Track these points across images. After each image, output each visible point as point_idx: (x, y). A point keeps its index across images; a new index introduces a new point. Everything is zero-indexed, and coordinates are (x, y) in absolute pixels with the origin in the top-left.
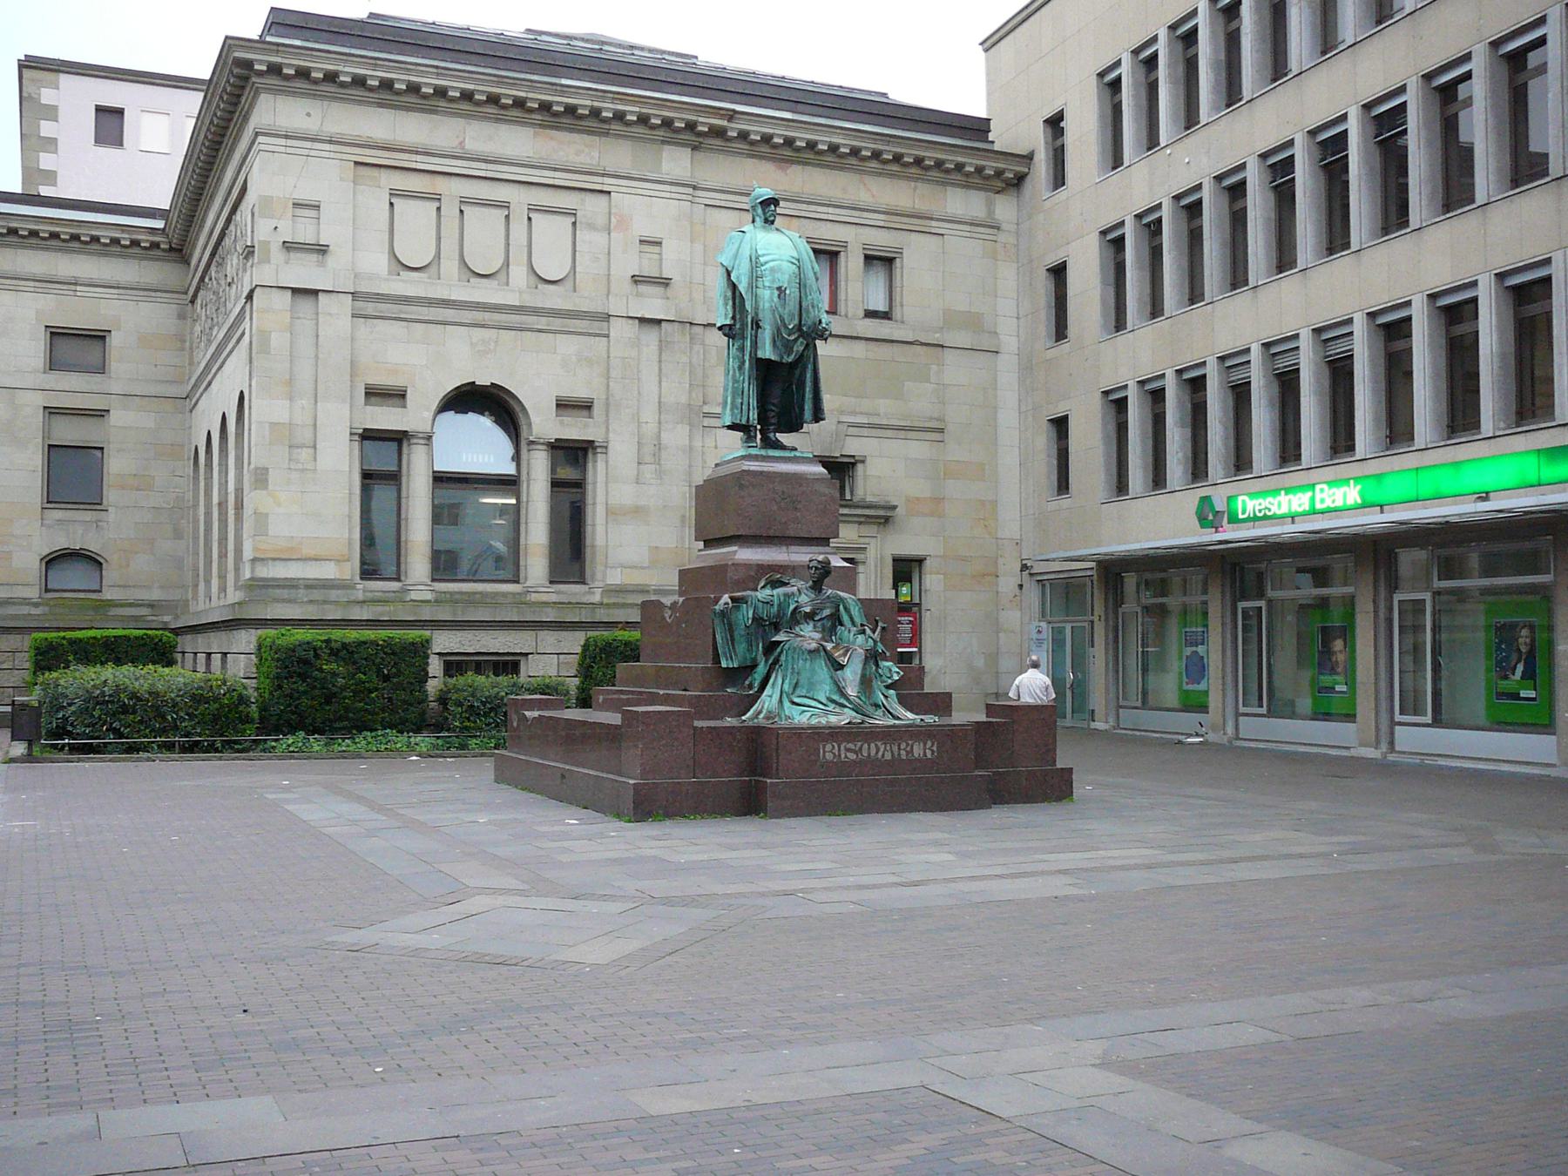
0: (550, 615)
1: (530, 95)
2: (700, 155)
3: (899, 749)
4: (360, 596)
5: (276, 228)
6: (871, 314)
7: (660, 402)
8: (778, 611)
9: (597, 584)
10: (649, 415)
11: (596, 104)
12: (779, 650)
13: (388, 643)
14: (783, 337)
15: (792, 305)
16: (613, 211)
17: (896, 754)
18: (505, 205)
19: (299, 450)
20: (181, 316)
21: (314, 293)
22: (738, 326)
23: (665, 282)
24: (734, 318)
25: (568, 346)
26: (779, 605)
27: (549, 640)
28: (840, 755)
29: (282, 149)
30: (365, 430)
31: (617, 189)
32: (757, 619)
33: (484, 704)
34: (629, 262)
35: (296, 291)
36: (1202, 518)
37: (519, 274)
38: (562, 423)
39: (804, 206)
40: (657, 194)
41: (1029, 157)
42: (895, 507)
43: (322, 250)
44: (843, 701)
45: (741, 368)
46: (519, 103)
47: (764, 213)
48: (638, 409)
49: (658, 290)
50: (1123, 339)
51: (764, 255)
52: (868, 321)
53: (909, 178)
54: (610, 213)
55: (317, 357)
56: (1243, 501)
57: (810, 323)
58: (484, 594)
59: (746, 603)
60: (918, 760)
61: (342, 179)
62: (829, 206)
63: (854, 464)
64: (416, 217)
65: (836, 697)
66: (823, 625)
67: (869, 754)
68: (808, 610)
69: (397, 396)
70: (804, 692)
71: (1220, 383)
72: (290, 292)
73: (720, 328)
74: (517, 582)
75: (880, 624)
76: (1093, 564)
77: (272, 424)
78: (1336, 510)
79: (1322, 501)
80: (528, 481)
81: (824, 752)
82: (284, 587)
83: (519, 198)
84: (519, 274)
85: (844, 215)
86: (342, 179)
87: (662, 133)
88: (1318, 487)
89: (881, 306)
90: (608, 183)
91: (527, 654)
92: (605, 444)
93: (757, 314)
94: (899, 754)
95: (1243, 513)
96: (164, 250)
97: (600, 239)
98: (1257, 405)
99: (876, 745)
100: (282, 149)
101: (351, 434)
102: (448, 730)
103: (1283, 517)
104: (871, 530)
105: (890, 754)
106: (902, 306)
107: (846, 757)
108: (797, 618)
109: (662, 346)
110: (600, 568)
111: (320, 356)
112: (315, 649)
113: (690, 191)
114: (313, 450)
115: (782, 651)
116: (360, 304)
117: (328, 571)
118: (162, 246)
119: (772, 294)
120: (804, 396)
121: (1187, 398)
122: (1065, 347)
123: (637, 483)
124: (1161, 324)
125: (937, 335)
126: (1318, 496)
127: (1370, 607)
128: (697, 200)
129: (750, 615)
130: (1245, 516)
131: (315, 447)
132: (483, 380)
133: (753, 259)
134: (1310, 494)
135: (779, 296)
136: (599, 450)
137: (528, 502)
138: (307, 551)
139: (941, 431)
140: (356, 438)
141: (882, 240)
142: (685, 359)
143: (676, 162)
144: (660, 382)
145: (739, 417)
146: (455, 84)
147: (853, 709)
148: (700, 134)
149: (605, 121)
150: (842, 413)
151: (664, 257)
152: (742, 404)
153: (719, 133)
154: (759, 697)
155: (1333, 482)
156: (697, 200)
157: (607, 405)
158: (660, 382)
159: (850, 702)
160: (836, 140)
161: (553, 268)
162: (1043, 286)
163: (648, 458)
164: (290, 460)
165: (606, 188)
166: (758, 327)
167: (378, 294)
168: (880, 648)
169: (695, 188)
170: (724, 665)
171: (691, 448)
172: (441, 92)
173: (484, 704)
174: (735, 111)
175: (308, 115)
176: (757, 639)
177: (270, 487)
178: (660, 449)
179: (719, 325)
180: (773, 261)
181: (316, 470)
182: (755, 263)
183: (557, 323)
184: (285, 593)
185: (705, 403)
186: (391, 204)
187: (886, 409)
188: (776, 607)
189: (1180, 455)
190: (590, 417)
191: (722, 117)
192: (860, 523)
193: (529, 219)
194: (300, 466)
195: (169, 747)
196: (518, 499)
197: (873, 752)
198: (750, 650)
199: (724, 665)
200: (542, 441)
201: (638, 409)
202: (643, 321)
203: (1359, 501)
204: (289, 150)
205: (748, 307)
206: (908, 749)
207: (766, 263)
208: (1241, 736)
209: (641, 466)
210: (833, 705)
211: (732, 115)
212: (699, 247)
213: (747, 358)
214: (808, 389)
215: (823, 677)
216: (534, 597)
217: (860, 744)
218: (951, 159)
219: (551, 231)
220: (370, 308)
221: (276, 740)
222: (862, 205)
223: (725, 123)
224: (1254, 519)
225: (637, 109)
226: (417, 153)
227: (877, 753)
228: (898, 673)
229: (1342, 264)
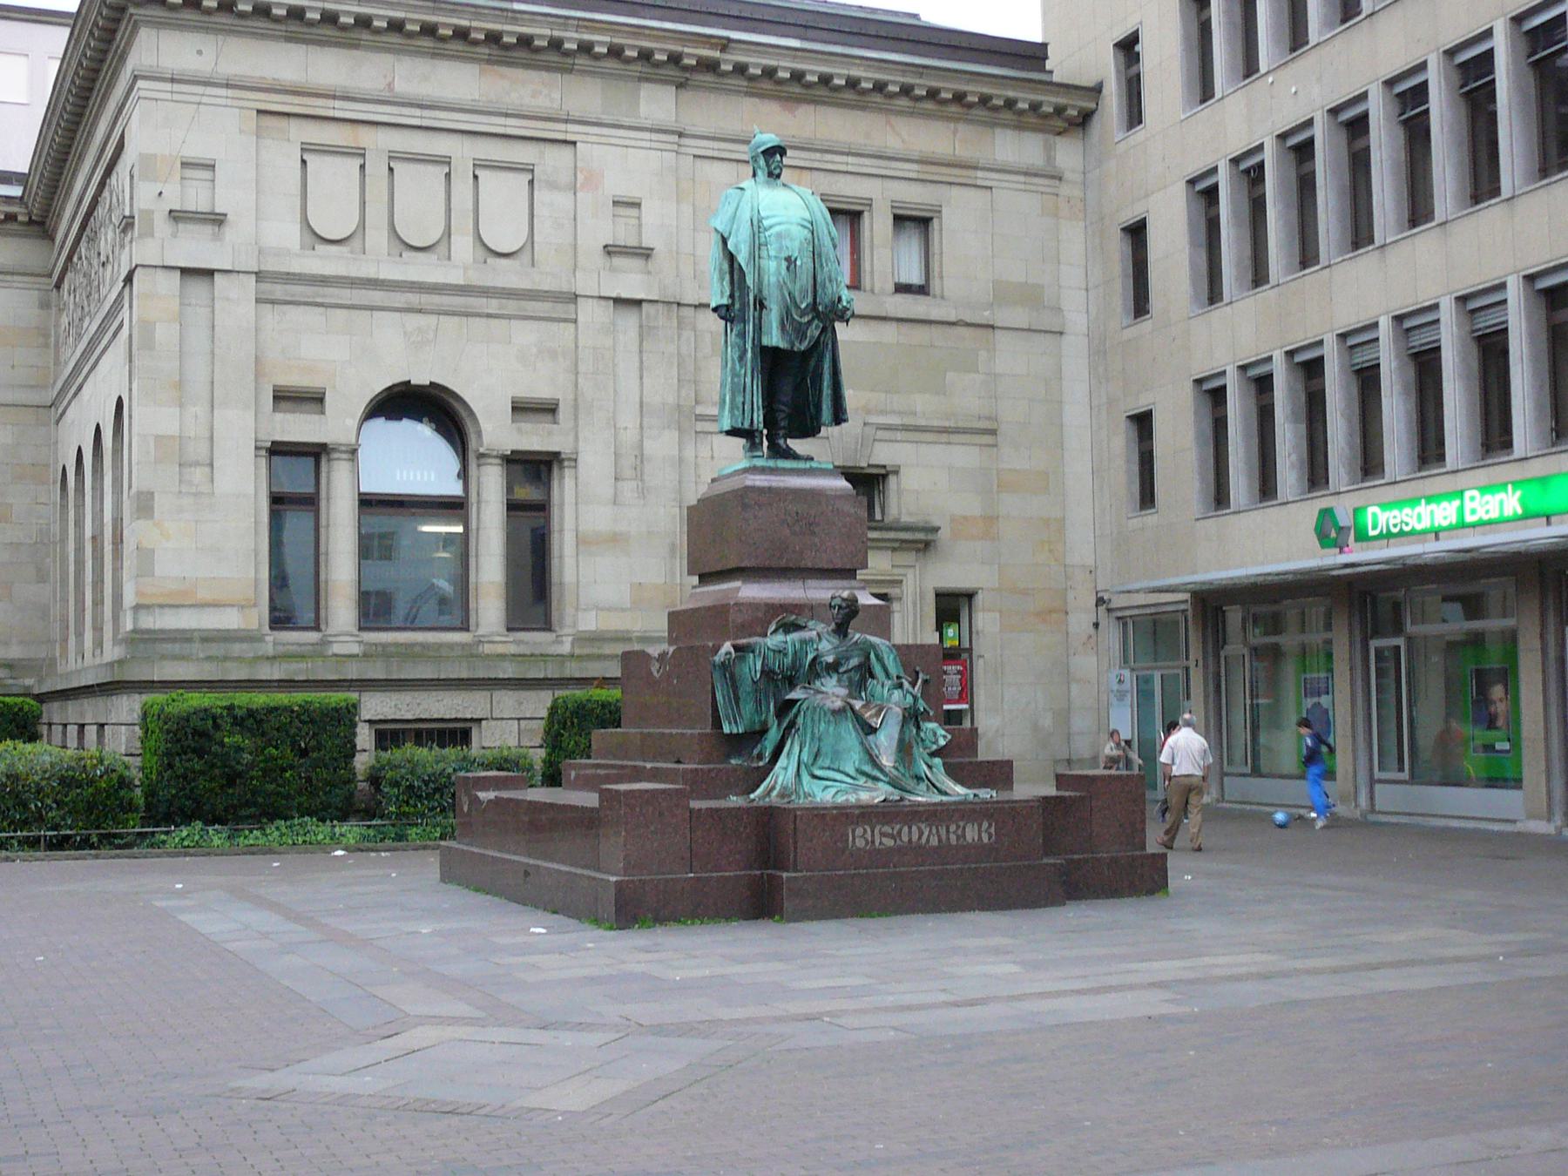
0: (508, 671)
1: (475, 24)
2: (687, 95)
3: (948, 831)
4: (270, 651)
5: (160, 193)
6: (902, 288)
9: (567, 631)
10: (628, 420)
11: (556, 33)
12: (794, 710)
13: (305, 708)
14: (794, 319)
15: (805, 279)
16: (579, 165)
17: (944, 837)
18: (445, 161)
19: (193, 469)
20: (45, 305)
21: (209, 273)
22: (737, 306)
23: (645, 253)
24: (732, 296)
25: (526, 335)
27: (507, 702)
28: (873, 842)
29: (168, 96)
30: (273, 442)
31: (584, 138)
32: (767, 673)
33: (426, 783)
34: (601, 229)
35: (186, 272)
36: (1322, 536)
37: (463, 245)
38: (519, 430)
39: (818, 156)
40: (633, 143)
41: (1097, 90)
42: (936, 529)
43: (217, 220)
45: (742, 358)
46: (462, 34)
47: (768, 165)
48: (614, 412)
49: (636, 263)
50: (1219, 314)
51: (768, 218)
52: (900, 298)
53: (948, 119)
54: (576, 167)
55: (213, 353)
56: (1374, 515)
57: (826, 300)
58: (424, 646)
59: (753, 652)
60: (969, 847)
61: (241, 132)
62: (848, 154)
63: (885, 476)
64: (337, 178)
65: (867, 768)
66: (850, 680)
67: (910, 840)
68: (830, 659)
69: (313, 400)
70: (827, 763)
71: (1342, 366)
72: (178, 273)
73: (715, 310)
74: (467, 629)
75: (921, 675)
76: (1187, 596)
77: (158, 438)
78: (1489, 523)
79: (1473, 512)
80: (479, 502)
81: (854, 839)
82: (174, 640)
83: (462, 152)
84: (463, 245)
85: (868, 165)
86: (241, 132)
87: (640, 69)
88: (1468, 494)
89: (916, 278)
90: (572, 131)
91: (479, 720)
92: (574, 456)
93: (760, 291)
95: (1374, 528)
96: (22, 223)
97: (563, 200)
98: (1389, 393)
100: (168, 96)
101: (257, 448)
102: (381, 817)
103: (1423, 533)
104: (908, 558)
105: (936, 838)
106: (941, 278)
107: (880, 843)
108: (817, 670)
109: (644, 332)
110: (569, 611)
111: (217, 351)
112: (214, 718)
113: (675, 138)
114: (207, 469)
115: (799, 711)
116: (265, 286)
117: (230, 620)
118: (20, 218)
119: (779, 265)
120: (821, 391)
121: (1300, 386)
122: (1146, 325)
124: (1265, 294)
125: (987, 313)
126: (1468, 505)
127: (1537, 644)
128: (683, 150)
129: (759, 667)
130: (1376, 533)
131: (211, 465)
132: (420, 378)
133: (755, 223)
134: (1457, 503)
135: (788, 268)
136: (566, 463)
137: (478, 529)
138: (203, 595)
139: (993, 432)
140: (263, 453)
141: (915, 196)
142: (672, 348)
143: (657, 103)
144: (641, 378)
145: (740, 420)
146: (381, 12)
147: (889, 783)
148: (686, 68)
149: (568, 53)
150: (869, 412)
151: (644, 222)
152: (744, 404)
153: (710, 66)
154: (772, 769)
155: (1484, 488)
156: (683, 150)
157: (576, 407)
158: (641, 378)
159: (886, 774)
160: (855, 72)
161: (505, 236)
162: (1118, 248)
163: (628, 473)
164: (180, 481)
165: (570, 137)
166: (762, 306)
167: (288, 274)
168: (922, 705)
169: (681, 135)
170: (726, 730)
171: (681, 460)
172: (364, 22)
173: (426, 783)
174: (729, 40)
175: (200, 52)
176: (767, 697)
177: (156, 515)
178: (642, 462)
179: (713, 305)
180: (780, 224)
181: (213, 493)
182: (757, 227)
183: (511, 306)
184: (176, 648)
185: (697, 402)
186: (304, 162)
187: (925, 406)
189: (1294, 457)
190: (555, 422)
191: (713, 47)
192: (894, 550)
193: (476, 177)
194: (193, 490)
195: (33, 843)
196: (466, 528)
197: (915, 837)
198: (758, 711)
199: (726, 730)
200: (495, 453)
202: (619, 301)
203: (1520, 512)
204: (176, 97)
205: (749, 281)
206: (959, 832)
207: (771, 227)
208: (1377, 808)
209: (620, 484)
210: (864, 779)
211: (725, 45)
212: (687, 209)
213: (749, 346)
214: (825, 384)
216: (487, 649)
217: (898, 827)
218: (1000, 94)
219: (502, 192)
220: (279, 291)
221: (167, 833)
222: (890, 153)
223: (717, 54)
224: (1387, 536)
225: (607, 39)
226: (334, 97)
227: (920, 838)
228: (945, 737)
229: (1491, 214)
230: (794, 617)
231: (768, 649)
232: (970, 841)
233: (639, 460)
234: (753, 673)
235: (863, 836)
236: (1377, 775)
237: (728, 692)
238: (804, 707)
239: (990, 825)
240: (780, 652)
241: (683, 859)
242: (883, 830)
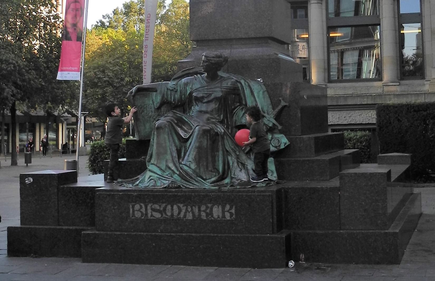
3: (200, 210)
8: (181, 96)
28: (146, 214)
59: (156, 91)
60: (215, 221)
67: (172, 215)
81: (133, 211)
94: (200, 215)
99: (179, 208)
105: (191, 214)
107: (152, 216)
147: (179, 175)
206: (208, 211)
217: (164, 205)
227: (179, 213)
231: (167, 89)
232: (216, 217)
235: (139, 210)
239: (231, 208)
240: (173, 90)
241: (53, 216)
242: (153, 207)
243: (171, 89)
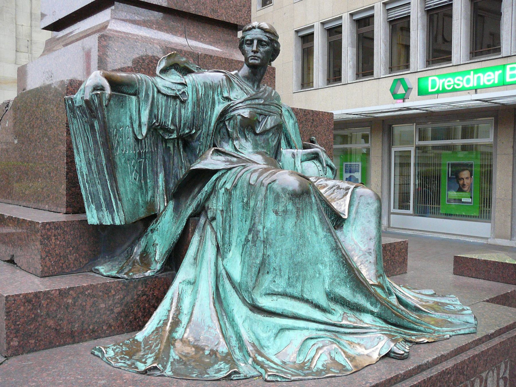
7: (31, 13)
12: (207, 188)
26: (197, 103)
36: (394, 94)
44: (360, 300)
48: (16, 15)
56: (434, 81)
68: (246, 113)
70: (281, 285)
71: (384, 19)
98: (415, 28)
123: (15, 64)
126: (508, 73)
129: (145, 118)
154: (167, 285)
163: (23, 49)
176: (154, 164)
178: (31, 44)
188: (190, 106)
189: (351, 63)
198: (142, 188)
201: (16, 15)
208: (391, 226)
209: (18, 54)
210: (339, 310)
215: (317, 249)
230: (184, 59)
231: (159, 92)
233: (29, 43)
234: (136, 126)
236: (392, 210)
237: (97, 155)
238: (228, 183)
243: (170, 93)
